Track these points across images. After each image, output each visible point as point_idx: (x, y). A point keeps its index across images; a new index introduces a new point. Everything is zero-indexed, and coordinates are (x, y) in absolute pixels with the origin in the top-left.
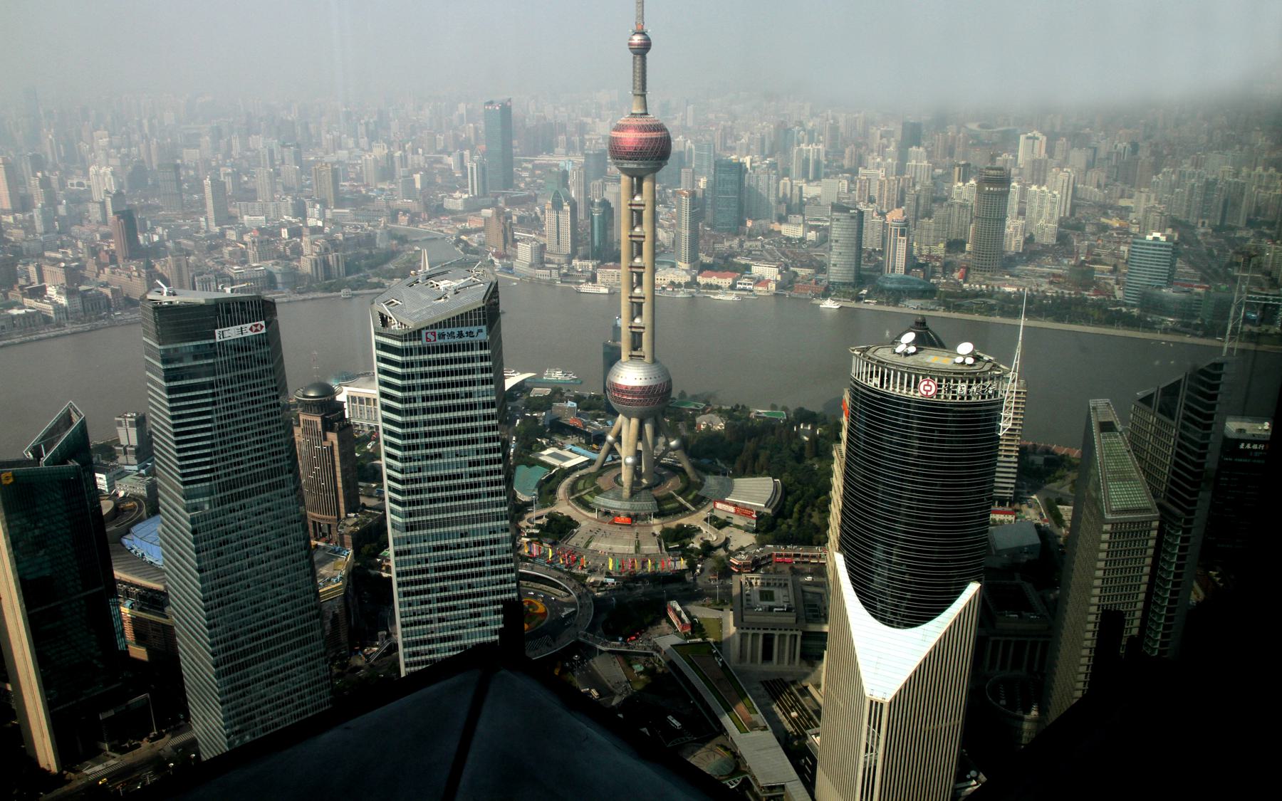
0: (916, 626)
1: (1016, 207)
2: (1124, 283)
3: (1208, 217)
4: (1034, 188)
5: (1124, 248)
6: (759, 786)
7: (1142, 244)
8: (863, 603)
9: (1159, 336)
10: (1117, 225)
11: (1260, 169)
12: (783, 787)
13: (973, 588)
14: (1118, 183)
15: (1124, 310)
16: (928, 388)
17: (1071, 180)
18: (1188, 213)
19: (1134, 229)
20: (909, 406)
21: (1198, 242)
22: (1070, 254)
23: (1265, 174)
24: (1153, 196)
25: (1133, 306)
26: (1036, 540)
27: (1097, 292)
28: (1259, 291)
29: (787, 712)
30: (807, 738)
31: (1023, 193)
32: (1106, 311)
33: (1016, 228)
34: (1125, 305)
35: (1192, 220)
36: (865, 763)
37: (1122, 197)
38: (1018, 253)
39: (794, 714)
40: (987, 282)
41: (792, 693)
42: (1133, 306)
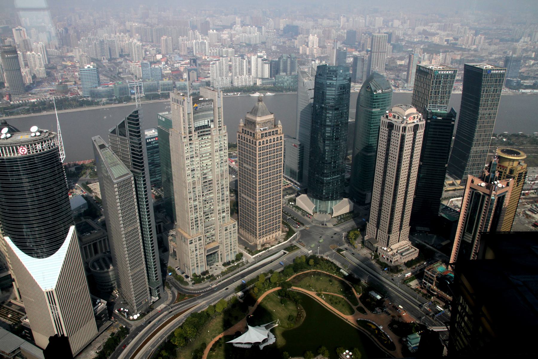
0: (54, 253)
1: (23, 63)
2: (81, 88)
3: (104, 56)
4: (28, 53)
5: (77, 74)
6: (7, 354)
7: (84, 70)
8: (26, 254)
9: (102, 107)
10: (70, 64)
11: (118, 34)
12: (19, 348)
13: (72, 229)
14: (64, 46)
15: (85, 99)
16: (23, 151)
17: (44, 48)
18: (96, 55)
19: (78, 65)
20: (17, 161)
21: (104, 66)
22: (55, 80)
23: (120, 36)
24: (81, 50)
25: (88, 97)
26: (85, 202)
27: (72, 94)
28: (133, 82)
29: (5, 317)
30: (21, 322)
31: (24, 56)
32: (78, 101)
33: (26, 72)
34: (85, 97)
35: (99, 58)
36: (54, 318)
37: (68, 52)
38: (31, 84)
39: (10, 316)
40: (21, 99)
41: (4, 308)
42: (88, 97)
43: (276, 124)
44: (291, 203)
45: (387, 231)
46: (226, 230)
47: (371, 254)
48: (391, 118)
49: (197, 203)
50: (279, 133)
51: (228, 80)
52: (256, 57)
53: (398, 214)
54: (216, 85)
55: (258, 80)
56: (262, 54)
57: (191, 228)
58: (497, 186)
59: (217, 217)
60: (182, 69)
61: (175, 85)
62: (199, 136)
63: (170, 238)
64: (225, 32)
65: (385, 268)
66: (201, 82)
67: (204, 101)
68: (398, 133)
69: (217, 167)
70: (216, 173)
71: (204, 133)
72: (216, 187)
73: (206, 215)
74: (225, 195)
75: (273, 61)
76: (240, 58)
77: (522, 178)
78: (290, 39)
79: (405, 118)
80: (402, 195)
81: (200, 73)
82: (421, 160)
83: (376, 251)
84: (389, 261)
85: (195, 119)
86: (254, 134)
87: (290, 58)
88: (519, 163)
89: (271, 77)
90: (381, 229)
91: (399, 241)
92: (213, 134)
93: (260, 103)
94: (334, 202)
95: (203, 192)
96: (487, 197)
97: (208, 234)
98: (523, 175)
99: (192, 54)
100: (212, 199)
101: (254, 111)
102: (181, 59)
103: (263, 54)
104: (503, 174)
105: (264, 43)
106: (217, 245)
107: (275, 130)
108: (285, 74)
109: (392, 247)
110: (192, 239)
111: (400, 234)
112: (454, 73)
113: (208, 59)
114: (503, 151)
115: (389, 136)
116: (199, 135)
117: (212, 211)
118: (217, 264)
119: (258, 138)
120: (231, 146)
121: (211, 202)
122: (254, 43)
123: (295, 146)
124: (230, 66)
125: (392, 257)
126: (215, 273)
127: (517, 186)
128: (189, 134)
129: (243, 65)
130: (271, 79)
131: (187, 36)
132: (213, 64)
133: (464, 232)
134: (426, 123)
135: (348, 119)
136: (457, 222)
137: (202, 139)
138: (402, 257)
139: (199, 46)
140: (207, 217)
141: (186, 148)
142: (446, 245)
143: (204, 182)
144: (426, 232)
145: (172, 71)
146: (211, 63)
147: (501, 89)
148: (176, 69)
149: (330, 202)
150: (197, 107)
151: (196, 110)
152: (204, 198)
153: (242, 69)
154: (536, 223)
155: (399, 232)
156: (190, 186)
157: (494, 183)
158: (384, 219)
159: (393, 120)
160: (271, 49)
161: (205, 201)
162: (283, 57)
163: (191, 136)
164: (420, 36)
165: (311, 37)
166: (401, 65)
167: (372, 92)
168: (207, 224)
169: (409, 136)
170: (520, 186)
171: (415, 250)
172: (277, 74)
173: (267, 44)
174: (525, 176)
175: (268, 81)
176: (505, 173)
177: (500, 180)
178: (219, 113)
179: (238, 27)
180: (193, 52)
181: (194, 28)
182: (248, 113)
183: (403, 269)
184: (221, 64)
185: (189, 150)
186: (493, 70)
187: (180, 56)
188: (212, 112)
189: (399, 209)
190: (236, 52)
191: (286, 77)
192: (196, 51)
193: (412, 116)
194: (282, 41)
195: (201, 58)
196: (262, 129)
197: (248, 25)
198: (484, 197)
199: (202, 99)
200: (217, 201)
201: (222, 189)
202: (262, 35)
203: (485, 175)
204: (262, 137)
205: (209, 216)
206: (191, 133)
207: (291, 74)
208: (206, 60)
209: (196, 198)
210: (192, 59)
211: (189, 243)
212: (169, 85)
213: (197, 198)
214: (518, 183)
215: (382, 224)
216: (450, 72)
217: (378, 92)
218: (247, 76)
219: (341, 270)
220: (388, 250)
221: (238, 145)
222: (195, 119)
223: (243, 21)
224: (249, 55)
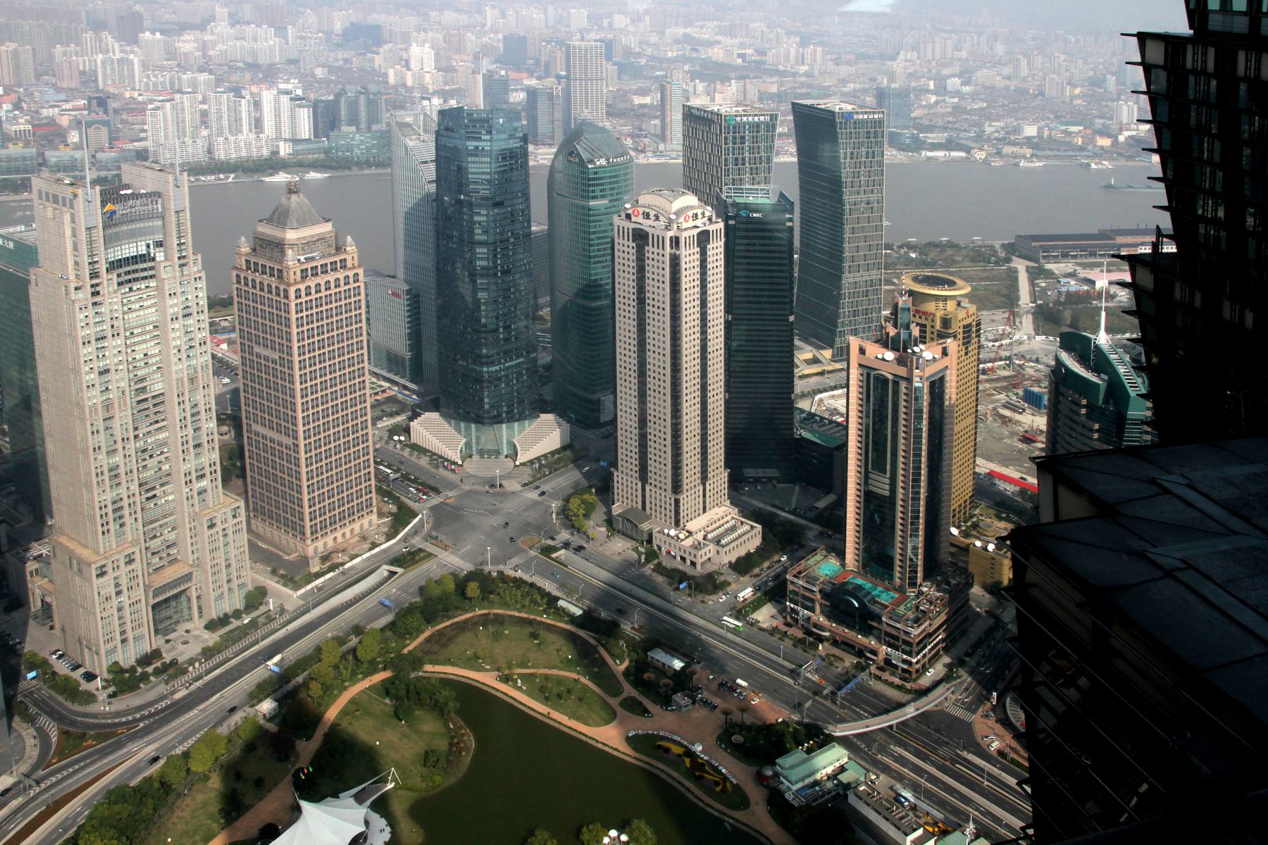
43: (340, 244)
44: (396, 438)
45: (669, 487)
46: (211, 526)
47: (636, 550)
48: (640, 219)
49: (117, 459)
50: (349, 264)
51: (199, 146)
52: (275, 92)
53: (692, 441)
54: (165, 157)
55: (282, 144)
56: (290, 87)
57: (100, 530)
58: (921, 357)
59: (181, 492)
60: (65, 121)
61: (44, 160)
62: (120, 284)
63: (31, 566)
64: (186, 37)
65: (680, 582)
66: (123, 150)
67: (135, 196)
68: (661, 252)
69: (176, 360)
70: (174, 376)
71: (137, 275)
72: (177, 410)
73: (147, 491)
74: (204, 431)
75: (322, 101)
76: (232, 94)
77: (974, 335)
78: (360, 54)
79: (673, 217)
80: (693, 395)
81: (119, 130)
82: (728, 309)
83: (650, 541)
84: (688, 563)
85: (108, 241)
86: (280, 271)
87: (366, 92)
88: (959, 304)
89: (316, 135)
90: (654, 483)
91: (704, 510)
92: (164, 276)
93: (294, 197)
94: (516, 424)
95: (136, 429)
96: (903, 385)
97: (155, 544)
98: (974, 329)
99: (93, 85)
100: (165, 444)
101: (276, 215)
102: (63, 96)
103: (294, 86)
104: (929, 329)
105: (291, 62)
106: (186, 571)
107: (337, 259)
108: (353, 129)
109: (691, 526)
110: (103, 563)
111: (704, 490)
112: (771, 120)
113: (140, 99)
114: (916, 279)
115: (641, 258)
116: (122, 279)
117: (165, 479)
118: (188, 626)
119: (292, 281)
120: (216, 304)
121: (162, 453)
122: (268, 61)
123: (394, 294)
124: (204, 114)
125: (693, 552)
126: (182, 653)
127: (966, 354)
128: (91, 278)
129: (240, 112)
130: (315, 142)
131: (77, 45)
132: (157, 109)
133: (867, 472)
134: (727, 226)
135: (529, 226)
137: (131, 289)
138: (720, 549)
139: (113, 69)
140: (150, 494)
141: (82, 316)
142: (826, 509)
143: (139, 402)
144: (770, 479)
145: (34, 126)
146: (150, 107)
147: (883, 152)
148: (45, 121)
149: (504, 426)
150: (114, 212)
151: (110, 220)
152: (140, 444)
153: (238, 120)
154: (1028, 436)
155: (701, 488)
156: (96, 414)
157: (913, 351)
158: (657, 458)
159: (646, 224)
160: (313, 75)
161: (144, 451)
162: (345, 93)
163: (97, 285)
164: (680, 46)
165: (415, 50)
166: (643, 106)
167: (582, 163)
168: (150, 515)
169: (690, 258)
170: (972, 353)
171: (752, 527)
172: (332, 130)
173: (301, 64)
174: (978, 331)
175: (310, 146)
176: (933, 327)
177: (924, 343)
178: (179, 225)
179: (222, 27)
180: (96, 80)
181: (98, 26)
182: (261, 221)
183: (730, 580)
184: (180, 110)
185: (91, 321)
186: (857, 113)
187: (58, 90)
188: (160, 223)
189: (692, 428)
190: (219, 81)
191: (358, 137)
192: (105, 80)
193: (690, 213)
194: (340, 56)
195: (123, 95)
196: (302, 258)
197: (248, 23)
198: (896, 384)
199: (129, 192)
200: (181, 448)
201: (193, 415)
202: (287, 43)
203: (888, 334)
204: (304, 278)
205: (158, 492)
206: (97, 277)
207: (369, 129)
208: (134, 99)
209: (116, 446)
210: (95, 98)
211: (94, 574)
212: (24, 159)
213: (120, 446)
214: (967, 348)
215: (654, 470)
216: (762, 118)
217: (598, 163)
218: (253, 136)
219: (561, 603)
220: (682, 536)
221: (236, 299)
222: (108, 241)
223: (236, 14)
224: (254, 89)
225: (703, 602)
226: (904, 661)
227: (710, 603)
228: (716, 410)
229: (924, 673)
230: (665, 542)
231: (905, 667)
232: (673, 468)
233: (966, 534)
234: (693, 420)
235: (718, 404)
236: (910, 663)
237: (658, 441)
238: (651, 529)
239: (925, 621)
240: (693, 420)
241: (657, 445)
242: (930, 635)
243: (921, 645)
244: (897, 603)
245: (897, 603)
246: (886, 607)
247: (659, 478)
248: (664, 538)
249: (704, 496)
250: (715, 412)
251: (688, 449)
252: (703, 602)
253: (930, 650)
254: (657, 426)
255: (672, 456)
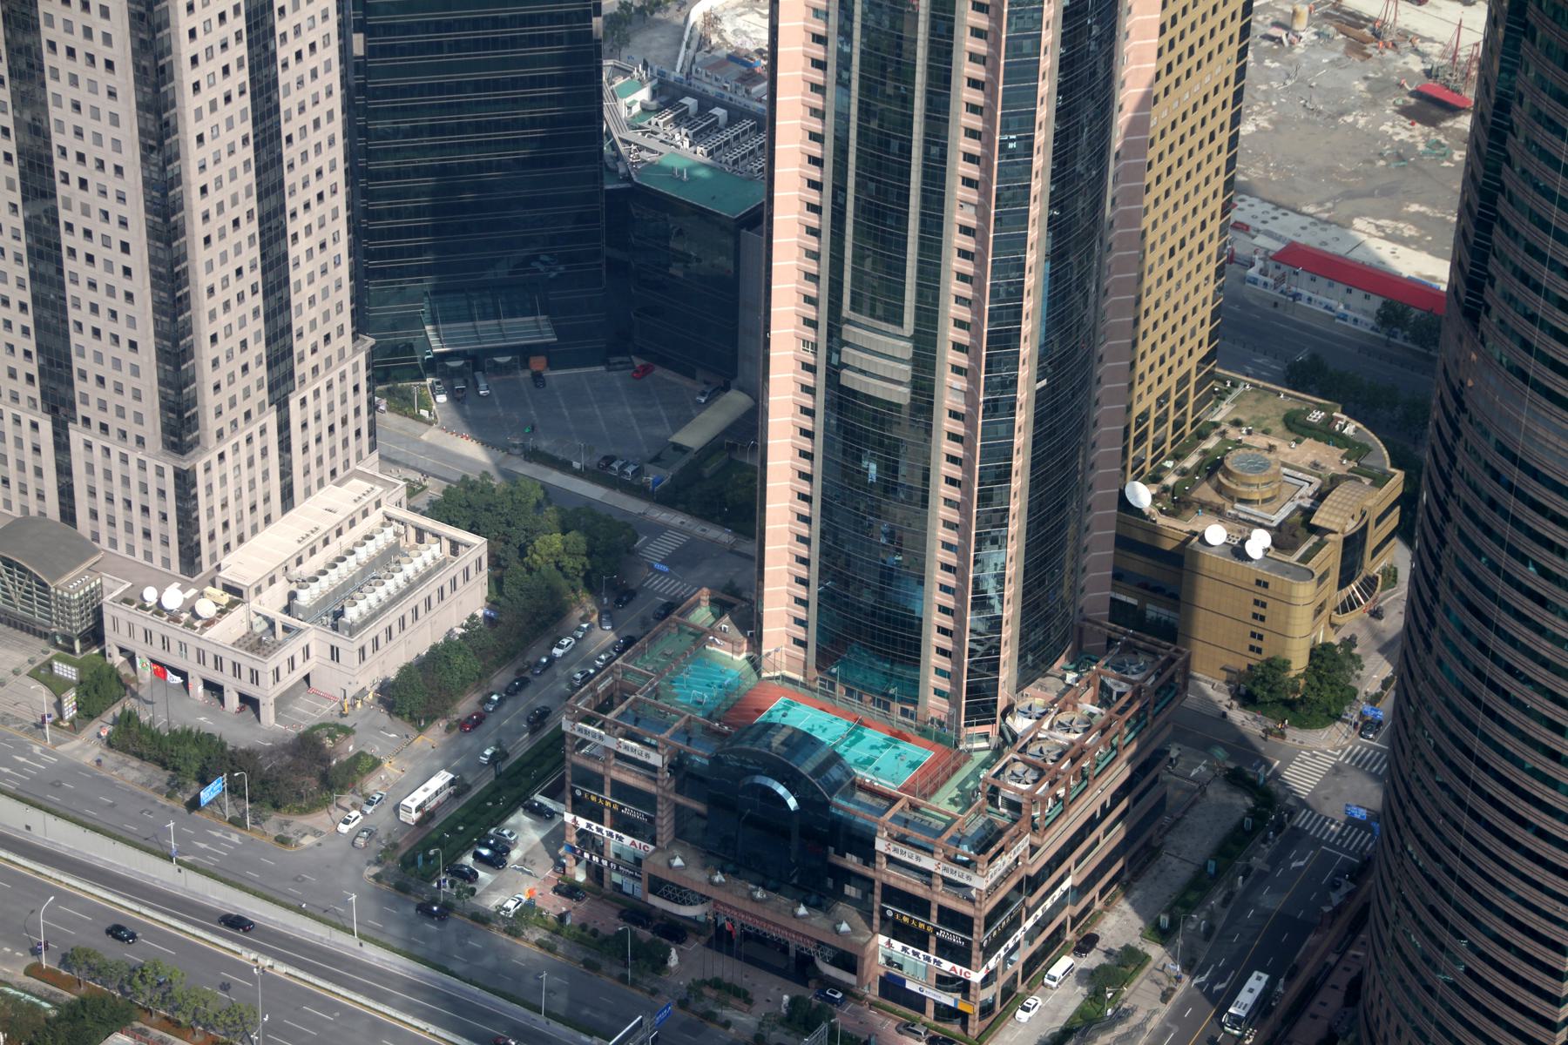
45: (152, 429)
47: (44, 674)
53: (228, 245)
65: (205, 782)
80: (221, 59)
83: (95, 636)
84: (233, 702)
90: (97, 417)
109: (241, 565)
111: (284, 426)
125: (247, 661)
136: (759, 219)
138: (338, 640)
142: (713, 447)
144: (525, 354)
154: (1433, 87)
155: (271, 419)
158: (102, 321)
171: (455, 546)
183: (375, 750)
189: (224, 195)
215: (93, 370)
220: (206, 608)
225: (283, 841)
226: (944, 982)
227: (308, 841)
228: (312, 113)
229: (1008, 1012)
230: (148, 635)
231: (948, 999)
232: (163, 355)
233: (1177, 502)
234: (228, 163)
235: (319, 86)
236: (964, 987)
237: (100, 254)
238: (96, 593)
239: (1017, 838)
240: (228, 163)
241: (97, 272)
242: (1031, 884)
243: (1002, 922)
244: (930, 781)
245: (930, 781)
246: (893, 800)
247: (113, 400)
248: (143, 620)
249: (285, 446)
250: (307, 119)
251: (215, 279)
252: (283, 841)
253: (1030, 937)
254: (91, 195)
255: (158, 308)
